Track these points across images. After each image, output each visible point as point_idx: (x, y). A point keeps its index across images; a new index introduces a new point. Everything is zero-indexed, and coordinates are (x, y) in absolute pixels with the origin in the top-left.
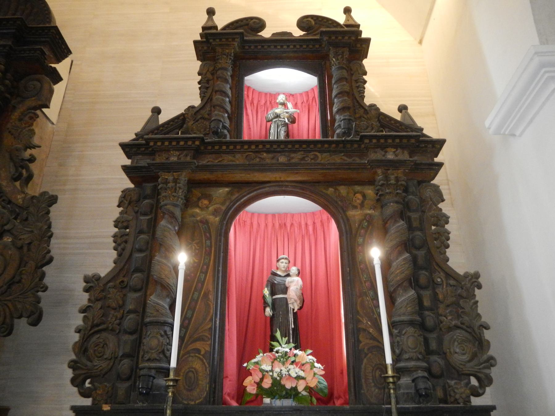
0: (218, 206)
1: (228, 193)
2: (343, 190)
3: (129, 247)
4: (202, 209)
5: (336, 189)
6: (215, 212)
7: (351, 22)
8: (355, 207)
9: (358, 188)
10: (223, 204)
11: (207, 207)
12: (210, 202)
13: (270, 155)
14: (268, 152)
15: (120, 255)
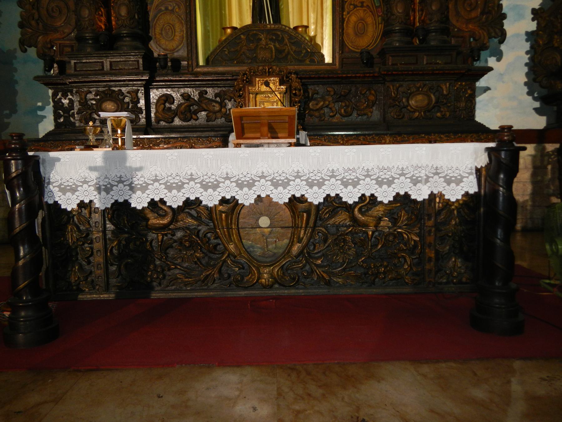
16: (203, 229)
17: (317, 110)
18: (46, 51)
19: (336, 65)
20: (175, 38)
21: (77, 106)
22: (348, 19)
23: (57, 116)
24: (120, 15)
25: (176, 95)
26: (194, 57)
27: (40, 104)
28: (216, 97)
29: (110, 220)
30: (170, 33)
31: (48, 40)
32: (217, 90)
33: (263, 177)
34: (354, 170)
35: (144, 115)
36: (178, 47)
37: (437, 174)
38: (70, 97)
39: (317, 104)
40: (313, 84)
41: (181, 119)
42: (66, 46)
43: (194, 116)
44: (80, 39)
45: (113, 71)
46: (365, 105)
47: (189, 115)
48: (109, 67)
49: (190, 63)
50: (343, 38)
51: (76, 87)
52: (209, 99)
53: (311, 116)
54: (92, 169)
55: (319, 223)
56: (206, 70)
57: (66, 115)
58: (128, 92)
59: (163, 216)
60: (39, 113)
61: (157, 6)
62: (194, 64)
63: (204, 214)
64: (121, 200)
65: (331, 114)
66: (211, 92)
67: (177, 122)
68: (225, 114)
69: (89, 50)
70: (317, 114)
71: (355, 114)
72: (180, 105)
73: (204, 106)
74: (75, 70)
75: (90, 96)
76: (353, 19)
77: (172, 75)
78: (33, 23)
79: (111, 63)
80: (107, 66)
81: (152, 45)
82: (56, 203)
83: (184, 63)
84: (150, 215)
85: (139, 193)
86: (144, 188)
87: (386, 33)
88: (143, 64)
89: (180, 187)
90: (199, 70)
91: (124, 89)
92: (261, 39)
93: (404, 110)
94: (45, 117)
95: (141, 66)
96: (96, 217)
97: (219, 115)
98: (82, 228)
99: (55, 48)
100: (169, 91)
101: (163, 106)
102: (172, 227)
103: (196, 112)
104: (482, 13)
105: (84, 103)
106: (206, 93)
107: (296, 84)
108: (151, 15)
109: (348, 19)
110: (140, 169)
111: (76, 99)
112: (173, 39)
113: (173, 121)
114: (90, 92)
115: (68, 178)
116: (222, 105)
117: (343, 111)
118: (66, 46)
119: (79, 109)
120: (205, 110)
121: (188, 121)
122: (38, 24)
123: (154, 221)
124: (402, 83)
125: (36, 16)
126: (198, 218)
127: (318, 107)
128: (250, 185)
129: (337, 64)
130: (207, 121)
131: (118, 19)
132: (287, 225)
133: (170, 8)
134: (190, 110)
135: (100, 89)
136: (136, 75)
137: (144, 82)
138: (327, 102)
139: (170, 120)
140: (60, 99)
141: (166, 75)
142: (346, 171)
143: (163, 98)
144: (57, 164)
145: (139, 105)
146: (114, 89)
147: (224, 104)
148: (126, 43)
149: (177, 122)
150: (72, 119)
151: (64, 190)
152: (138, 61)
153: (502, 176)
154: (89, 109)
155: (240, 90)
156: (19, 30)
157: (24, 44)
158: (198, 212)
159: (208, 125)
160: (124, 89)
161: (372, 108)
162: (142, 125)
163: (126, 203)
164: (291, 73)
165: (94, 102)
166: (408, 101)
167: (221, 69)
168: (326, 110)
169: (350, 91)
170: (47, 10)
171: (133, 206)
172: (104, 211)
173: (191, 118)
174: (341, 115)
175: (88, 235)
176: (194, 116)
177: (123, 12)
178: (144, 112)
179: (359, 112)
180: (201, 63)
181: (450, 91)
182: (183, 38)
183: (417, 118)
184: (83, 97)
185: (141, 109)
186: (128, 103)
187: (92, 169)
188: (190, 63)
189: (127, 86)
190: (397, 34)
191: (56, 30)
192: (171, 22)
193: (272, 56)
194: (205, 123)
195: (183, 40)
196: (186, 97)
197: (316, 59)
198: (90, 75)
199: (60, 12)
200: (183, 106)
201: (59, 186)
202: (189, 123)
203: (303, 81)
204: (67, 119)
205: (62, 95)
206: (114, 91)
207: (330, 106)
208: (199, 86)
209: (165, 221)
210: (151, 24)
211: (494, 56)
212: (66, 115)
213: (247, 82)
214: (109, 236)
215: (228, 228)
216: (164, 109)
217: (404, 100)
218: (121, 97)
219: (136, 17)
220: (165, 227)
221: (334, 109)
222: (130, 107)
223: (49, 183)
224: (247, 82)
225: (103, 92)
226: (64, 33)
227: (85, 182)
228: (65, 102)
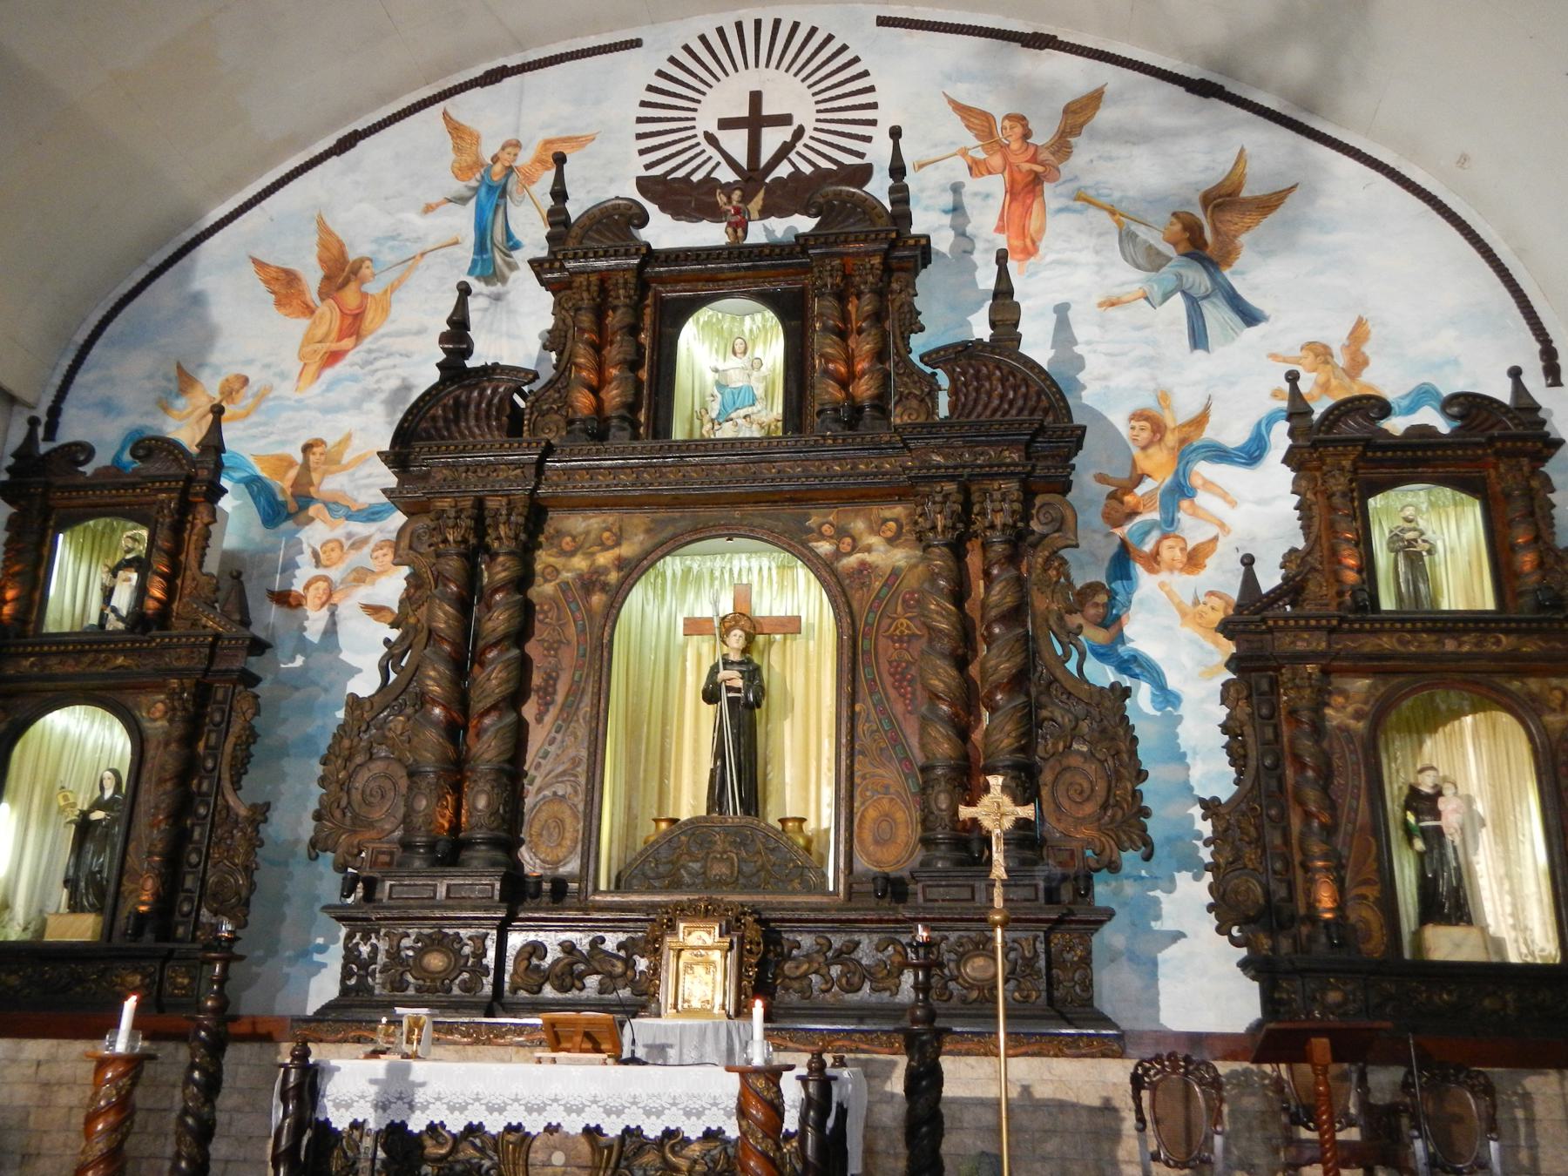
0: (1360, 705)
1: (1370, 687)
2: (1534, 684)
3: (1252, 763)
4: (1337, 710)
5: (1524, 683)
6: (1358, 715)
7: (1524, 403)
8: (1554, 710)
9: (1555, 682)
10: (1366, 702)
11: (1344, 707)
12: (1347, 698)
13: (1433, 638)
14: (1429, 631)
15: (1240, 773)
16: (487, 1163)
17: (797, 978)
18: (350, 859)
19: (838, 895)
20: (564, 843)
21: (382, 958)
22: (863, 816)
23: (346, 973)
24: (476, 809)
25: (552, 940)
26: (591, 878)
27: (320, 941)
28: (619, 949)
29: (383, 1147)
30: (555, 835)
31: (356, 842)
32: (622, 937)
33: (556, 1100)
34: (659, 1096)
35: (491, 978)
36: (565, 857)
37: (634, 1103)
38: (374, 940)
39: (797, 968)
40: (792, 931)
41: (554, 987)
42: (384, 853)
43: (578, 984)
44: (407, 845)
45: (450, 902)
46: (885, 972)
47: (568, 981)
48: (444, 894)
49: (583, 886)
50: (851, 847)
51: (385, 926)
52: (606, 952)
53: (787, 989)
54: (373, 1082)
55: (623, 1163)
56: (609, 898)
57: (361, 972)
58: (470, 938)
59: (441, 1145)
60: (317, 957)
61: (540, 790)
62: (590, 889)
63: (490, 1144)
64: (397, 1121)
65: (823, 987)
66: (612, 941)
67: (549, 992)
68: (632, 981)
69: (417, 863)
70: (796, 985)
71: (867, 987)
72: (556, 962)
73: (596, 965)
74: (390, 897)
75: (406, 942)
76: (872, 814)
77: (547, 910)
78: (338, 814)
79: (449, 887)
80: (442, 891)
81: (524, 853)
82: (327, 1120)
83: (573, 886)
84: (429, 1142)
85: (418, 1113)
86: (424, 1108)
87: (926, 842)
88: (502, 891)
89: (463, 1108)
90: (597, 898)
91: (463, 932)
92: (715, 842)
93: (952, 985)
94: (324, 965)
95: (497, 893)
96: (368, 1142)
97: (620, 982)
98: (350, 1154)
99: (363, 855)
100: (541, 937)
101: (526, 963)
102: (450, 1159)
103: (581, 976)
104: (1105, 807)
105: (394, 954)
106: (603, 940)
107: (753, 932)
108: (529, 801)
109: (863, 816)
110: (422, 1085)
111: (383, 946)
112: (559, 845)
113: (540, 991)
114: (408, 936)
115: (345, 1091)
116: (629, 963)
117: (844, 981)
118: (384, 853)
119: (385, 965)
120: (597, 973)
121: (567, 991)
122: (344, 814)
123: (432, 1150)
124: (946, 933)
125: (344, 803)
126: (481, 1150)
127: (798, 973)
128: (541, 1109)
129: (842, 895)
130: (600, 992)
131: (470, 815)
132: (585, 1164)
133: (560, 793)
134: (572, 973)
135: (426, 931)
136: (487, 909)
137: (497, 922)
138: (816, 965)
139: (535, 989)
140: (358, 944)
141: (537, 910)
142: (650, 1097)
143: (529, 949)
144: (336, 1074)
145: (485, 961)
146: (446, 930)
147: (631, 963)
148: (479, 854)
149: (549, 992)
150: (370, 979)
151: (337, 1106)
152: (493, 886)
153: (812, 1113)
154: (401, 965)
155: (656, 941)
156: (314, 823)
157: (316, 846)
158: (482, 1142)
159: (601, 999)
160: (463, 932)
161: (898, 977)
162: (487, 997)
163: (403, 1125)
164: (744, 914)
165: (411, 953)
166: (959, 970)
167: (635, 898)
168: (813, 977)
169: (858, 944)
170: (363, 792)
171: (409, 1128)
172: (378, 1133)
173: (573, 986)
174: (841, 988)
175: (354, 1163)
176: (578, 984)
177: (482, 802)
178: (492, 972)
179: (874, 985)
180: (603, 886)
181: (1036, 951)
182: (576, 843)
183: (975, 1000)
184: (395, 943)
185: (487, 968)
186: (467, 957)
187: (373, 1082)
188: (583, 886)
189: (470, 926)
190: (943, 847)
191: (371, 825)
192: (560, 816)
193: (732, 873)
194: (598, 996)
195: (575, 847)
196: (569, 948)
197: (812, 877)
198: (411, 907)
199: (383, 797)
200: (561, 964)
201: (334, 1101)
202: (569, 995)
203: (772, 924)
204: (361, 979)
205: (362, 939)
206: (447, 934)
207: (823, 971)
208: (592, 929)
209: (443, 1151)
210: (526, 818)
211: (1188, 870)
212: (361, 972)
213: (668, 927)
214: (378, 1165)
215: (514, 1164)
216: (527, 968)
217: (952, 965)
218: (456, 946)
219: (501, 811)
220: (443, 1158)
221: (828, 977)
222: (470, 963)
223: (323, 1096)
224: (668, 927)
225: (429, 936)
226: (383, 830)
227: (362, 1097)
228: (365, 950)
